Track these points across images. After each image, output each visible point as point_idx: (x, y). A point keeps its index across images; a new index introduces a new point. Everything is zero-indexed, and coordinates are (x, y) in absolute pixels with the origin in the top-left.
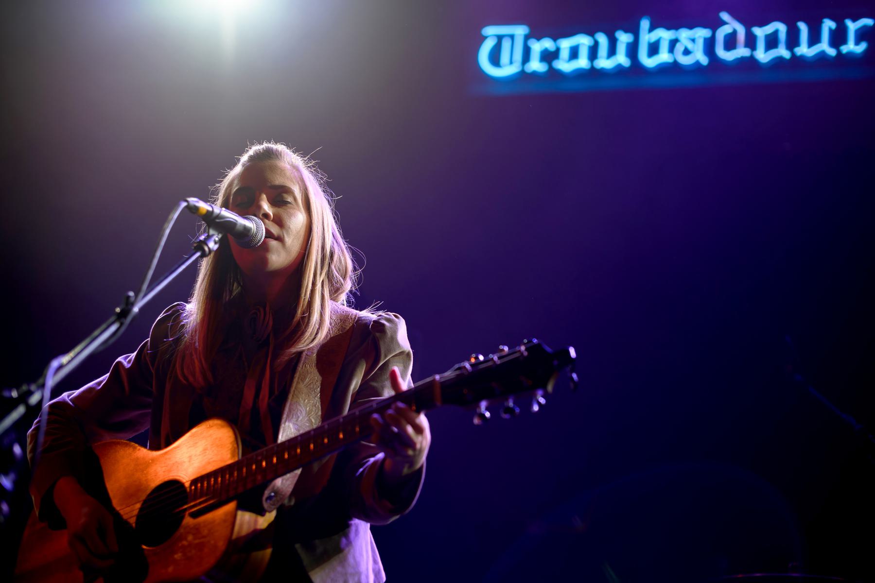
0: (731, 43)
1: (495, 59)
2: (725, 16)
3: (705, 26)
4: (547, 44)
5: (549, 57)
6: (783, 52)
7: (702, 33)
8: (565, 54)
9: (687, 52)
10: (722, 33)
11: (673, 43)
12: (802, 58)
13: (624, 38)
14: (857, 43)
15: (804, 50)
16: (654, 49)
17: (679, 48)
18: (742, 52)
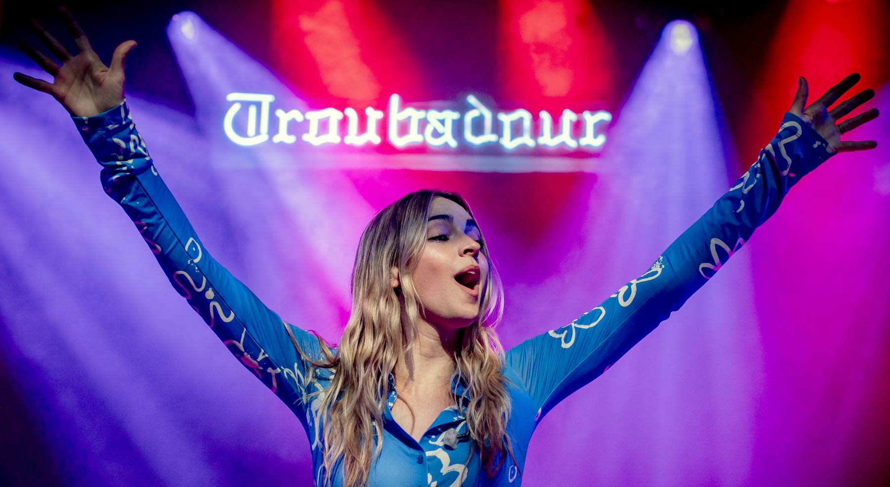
0: (478, 127)
1: (240, 127)
2: (472, 99)
3: (454, 109)
4: (296, 115)
5: (296, 128)
6: (527, 140)
7: (450, 116)
8: (314, 127)
9: (436, 134)
10: (470, 116)
11: (423, 123)
12: (545, 145)
13: (374, 115)
14: (595, 136)
15: (547, 140)
16: (404, 129)
17: (429, 130)
18: (489, 137)
